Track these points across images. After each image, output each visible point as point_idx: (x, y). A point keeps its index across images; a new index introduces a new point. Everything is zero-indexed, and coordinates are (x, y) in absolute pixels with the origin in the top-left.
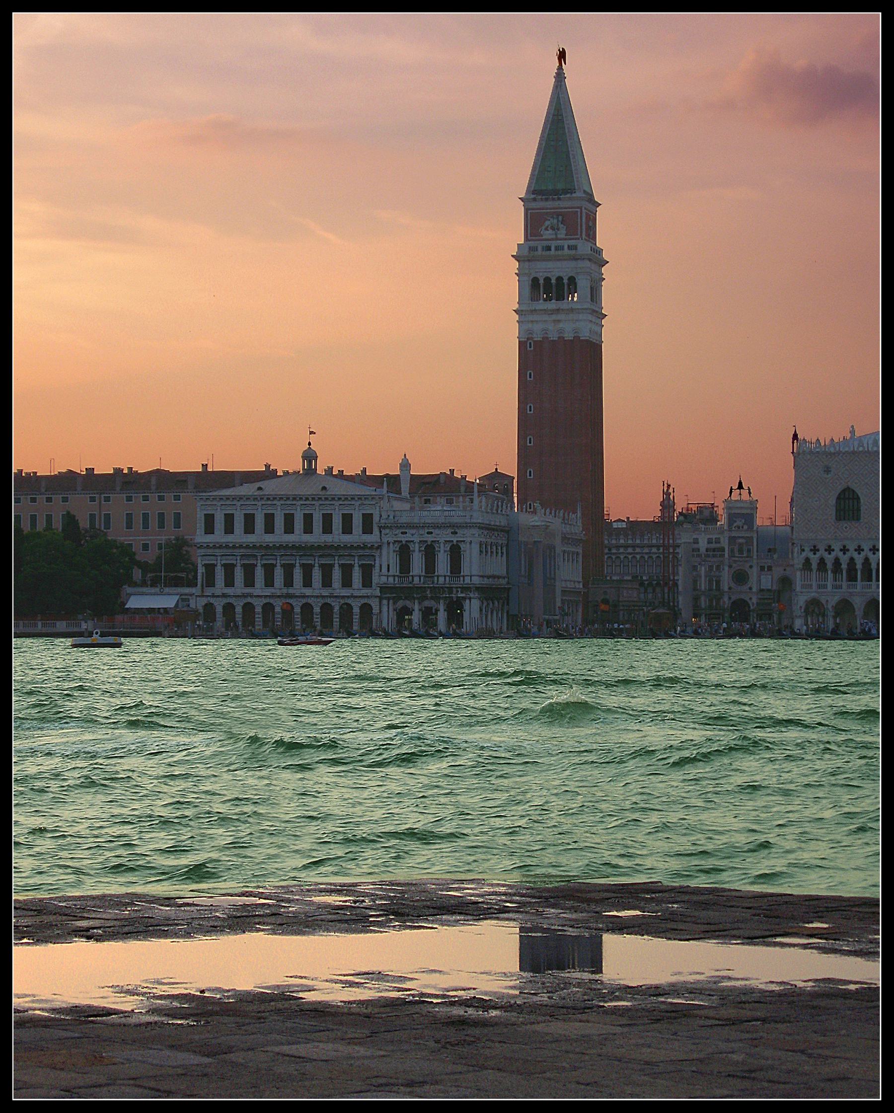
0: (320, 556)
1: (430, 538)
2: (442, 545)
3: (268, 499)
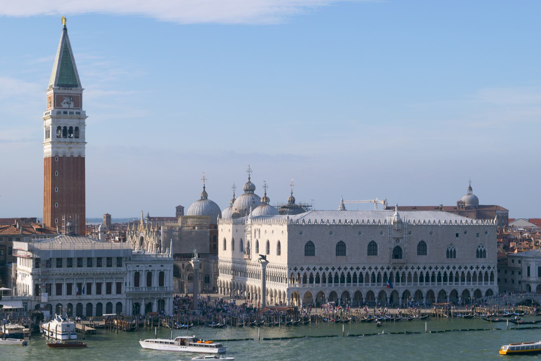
0: (96, 279)
1: (150, 269)
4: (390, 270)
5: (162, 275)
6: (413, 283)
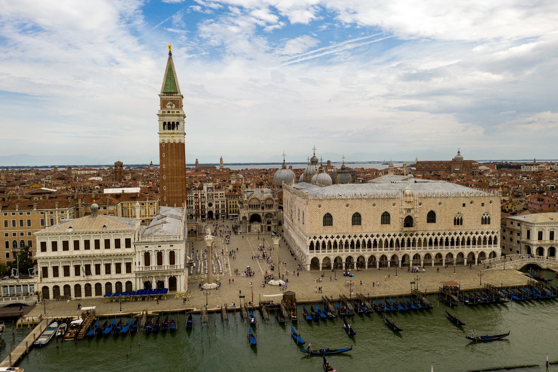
0: (104, 260)
1: (159, 249)
3: (76, 234)
4: (402, 237)
6: (422, 247)
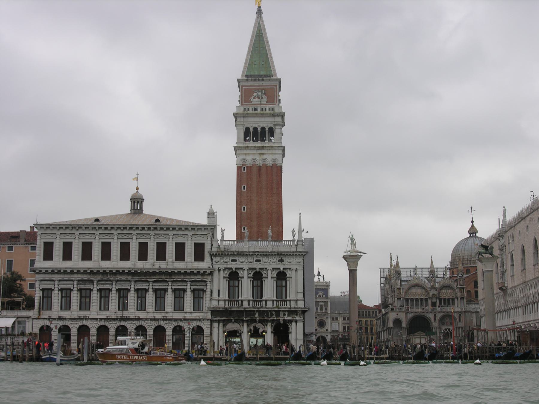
1: (258, 266)
2: (269, 272)
5: (281, 276)
